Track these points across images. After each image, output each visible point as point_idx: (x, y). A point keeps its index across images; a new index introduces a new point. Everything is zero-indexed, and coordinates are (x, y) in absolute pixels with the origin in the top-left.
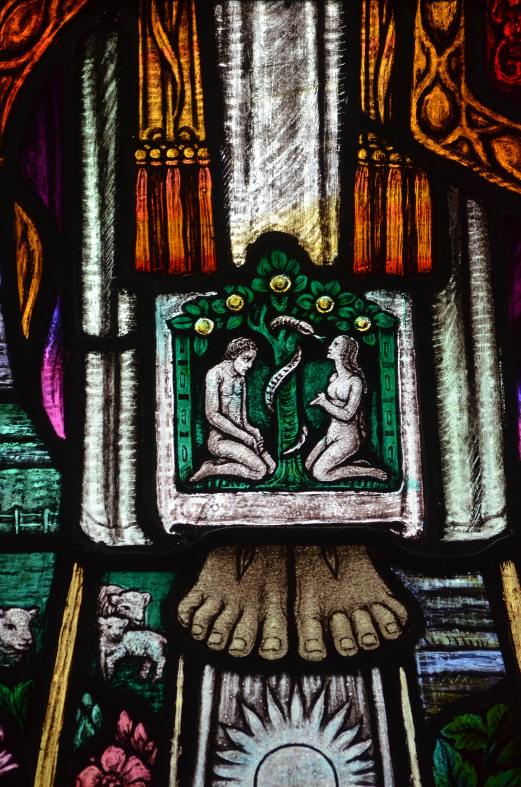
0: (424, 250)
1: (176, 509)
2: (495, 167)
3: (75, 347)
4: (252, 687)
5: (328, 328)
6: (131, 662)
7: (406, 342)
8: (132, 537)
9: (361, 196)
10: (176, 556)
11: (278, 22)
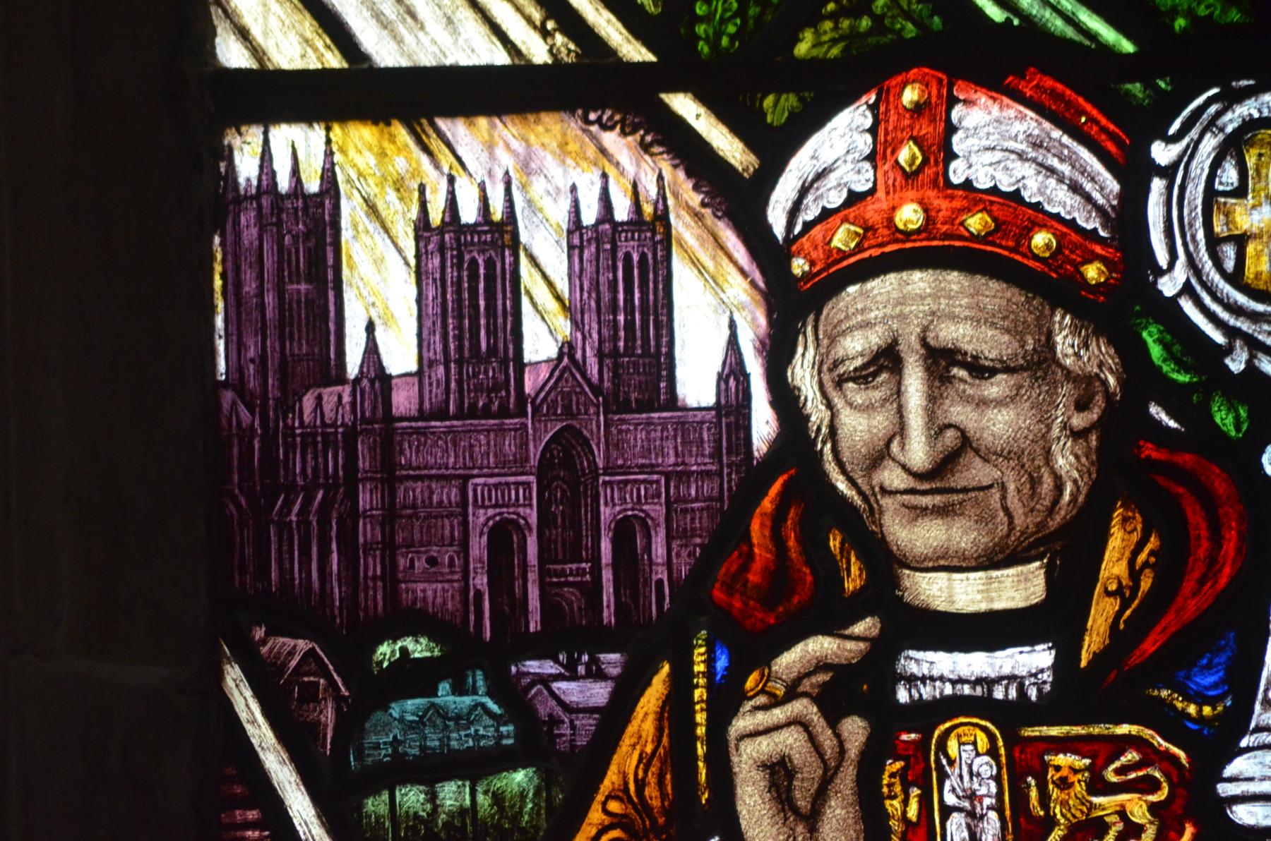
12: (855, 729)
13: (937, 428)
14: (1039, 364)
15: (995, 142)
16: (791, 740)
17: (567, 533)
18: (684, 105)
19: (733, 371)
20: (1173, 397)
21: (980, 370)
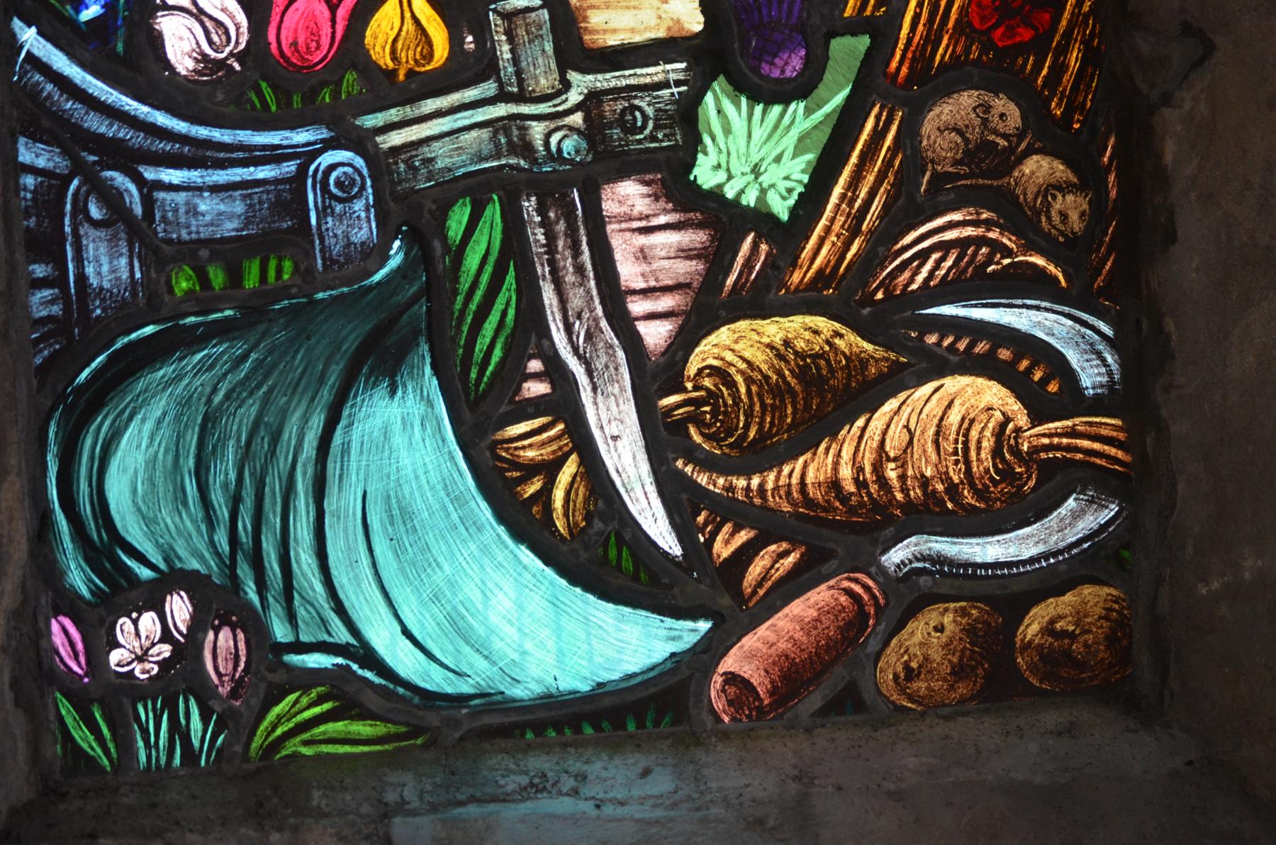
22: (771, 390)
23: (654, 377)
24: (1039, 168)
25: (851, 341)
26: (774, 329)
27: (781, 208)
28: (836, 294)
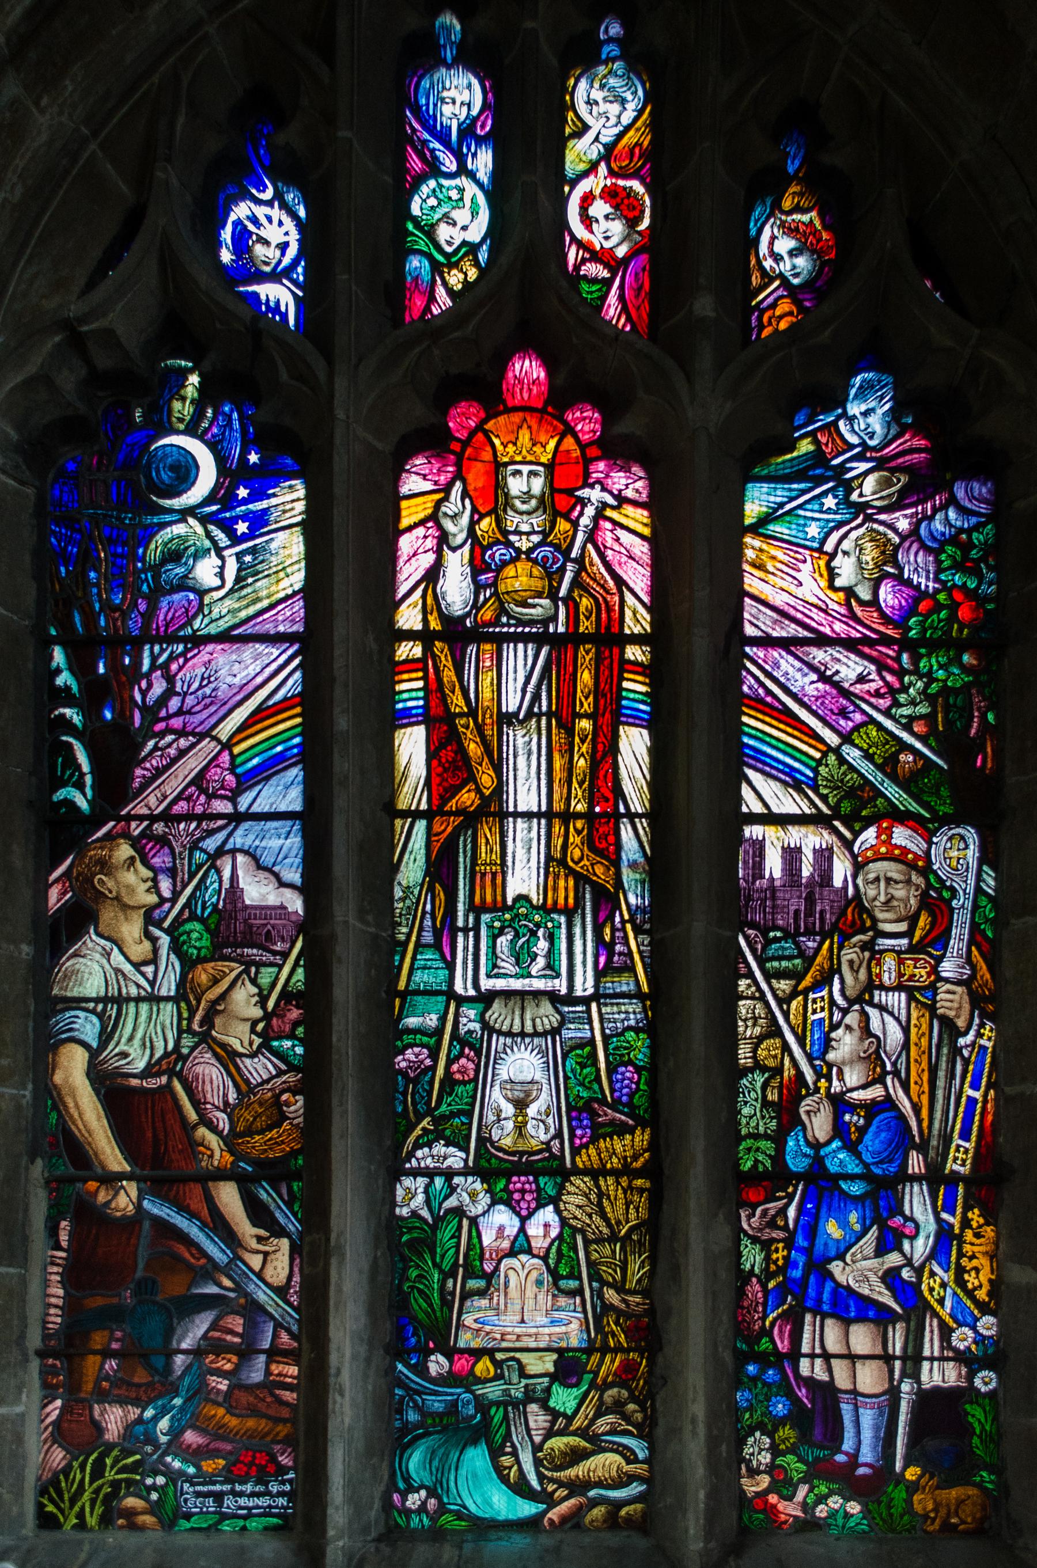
0: (571, 901)
1: (486, 984)
2: (595, 875)
3: (454, 931)
4: (509, 1041)
5: (538, 925)
6: (470, 1032)
7: (564, 930)
8: (472, 992)
9: (550, 883)
10: (486, 999)
11: (526, 825)
12: (867, 954)
13: (887, 894)
14: (908, 882)
15: (901, 836)
16: (854, 956)
17: (810, 912)
18: (836, 823)
19: (846, 880)
20: (935, 890)
21: (896, 882)
22: (563, 1454)
23: (537, 1448)
24: (631, 1407)
25: (584, 1444)
26: (566, 1439)
27: (569, 1412)
28: (582, 1433)
